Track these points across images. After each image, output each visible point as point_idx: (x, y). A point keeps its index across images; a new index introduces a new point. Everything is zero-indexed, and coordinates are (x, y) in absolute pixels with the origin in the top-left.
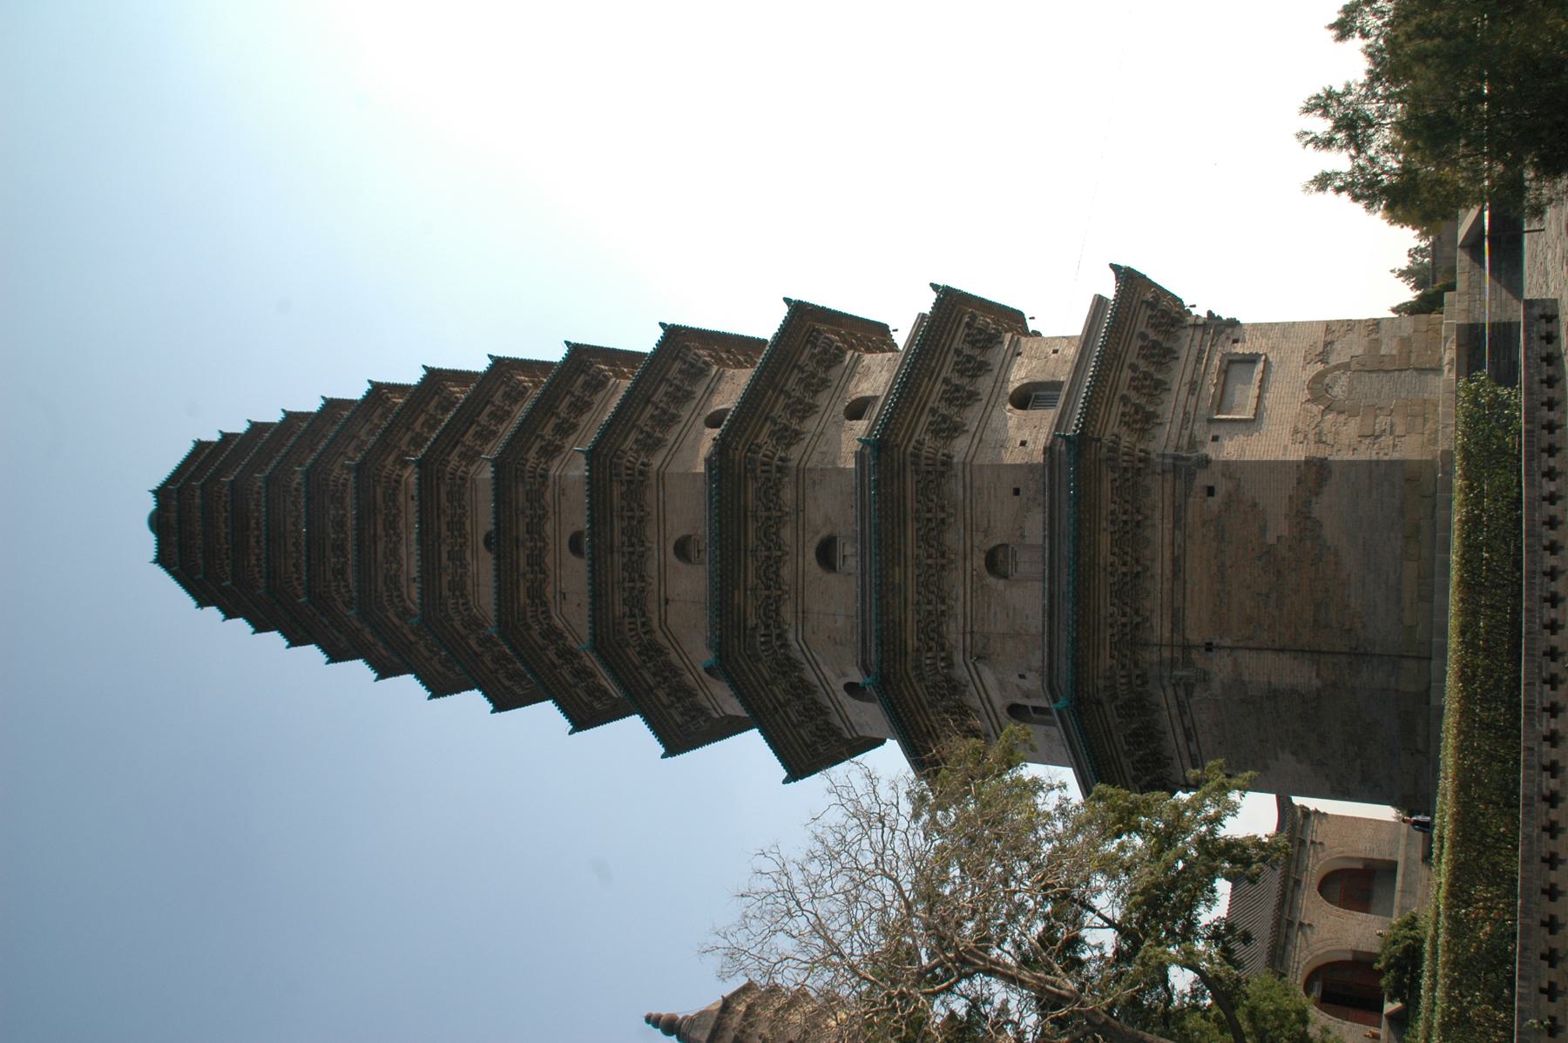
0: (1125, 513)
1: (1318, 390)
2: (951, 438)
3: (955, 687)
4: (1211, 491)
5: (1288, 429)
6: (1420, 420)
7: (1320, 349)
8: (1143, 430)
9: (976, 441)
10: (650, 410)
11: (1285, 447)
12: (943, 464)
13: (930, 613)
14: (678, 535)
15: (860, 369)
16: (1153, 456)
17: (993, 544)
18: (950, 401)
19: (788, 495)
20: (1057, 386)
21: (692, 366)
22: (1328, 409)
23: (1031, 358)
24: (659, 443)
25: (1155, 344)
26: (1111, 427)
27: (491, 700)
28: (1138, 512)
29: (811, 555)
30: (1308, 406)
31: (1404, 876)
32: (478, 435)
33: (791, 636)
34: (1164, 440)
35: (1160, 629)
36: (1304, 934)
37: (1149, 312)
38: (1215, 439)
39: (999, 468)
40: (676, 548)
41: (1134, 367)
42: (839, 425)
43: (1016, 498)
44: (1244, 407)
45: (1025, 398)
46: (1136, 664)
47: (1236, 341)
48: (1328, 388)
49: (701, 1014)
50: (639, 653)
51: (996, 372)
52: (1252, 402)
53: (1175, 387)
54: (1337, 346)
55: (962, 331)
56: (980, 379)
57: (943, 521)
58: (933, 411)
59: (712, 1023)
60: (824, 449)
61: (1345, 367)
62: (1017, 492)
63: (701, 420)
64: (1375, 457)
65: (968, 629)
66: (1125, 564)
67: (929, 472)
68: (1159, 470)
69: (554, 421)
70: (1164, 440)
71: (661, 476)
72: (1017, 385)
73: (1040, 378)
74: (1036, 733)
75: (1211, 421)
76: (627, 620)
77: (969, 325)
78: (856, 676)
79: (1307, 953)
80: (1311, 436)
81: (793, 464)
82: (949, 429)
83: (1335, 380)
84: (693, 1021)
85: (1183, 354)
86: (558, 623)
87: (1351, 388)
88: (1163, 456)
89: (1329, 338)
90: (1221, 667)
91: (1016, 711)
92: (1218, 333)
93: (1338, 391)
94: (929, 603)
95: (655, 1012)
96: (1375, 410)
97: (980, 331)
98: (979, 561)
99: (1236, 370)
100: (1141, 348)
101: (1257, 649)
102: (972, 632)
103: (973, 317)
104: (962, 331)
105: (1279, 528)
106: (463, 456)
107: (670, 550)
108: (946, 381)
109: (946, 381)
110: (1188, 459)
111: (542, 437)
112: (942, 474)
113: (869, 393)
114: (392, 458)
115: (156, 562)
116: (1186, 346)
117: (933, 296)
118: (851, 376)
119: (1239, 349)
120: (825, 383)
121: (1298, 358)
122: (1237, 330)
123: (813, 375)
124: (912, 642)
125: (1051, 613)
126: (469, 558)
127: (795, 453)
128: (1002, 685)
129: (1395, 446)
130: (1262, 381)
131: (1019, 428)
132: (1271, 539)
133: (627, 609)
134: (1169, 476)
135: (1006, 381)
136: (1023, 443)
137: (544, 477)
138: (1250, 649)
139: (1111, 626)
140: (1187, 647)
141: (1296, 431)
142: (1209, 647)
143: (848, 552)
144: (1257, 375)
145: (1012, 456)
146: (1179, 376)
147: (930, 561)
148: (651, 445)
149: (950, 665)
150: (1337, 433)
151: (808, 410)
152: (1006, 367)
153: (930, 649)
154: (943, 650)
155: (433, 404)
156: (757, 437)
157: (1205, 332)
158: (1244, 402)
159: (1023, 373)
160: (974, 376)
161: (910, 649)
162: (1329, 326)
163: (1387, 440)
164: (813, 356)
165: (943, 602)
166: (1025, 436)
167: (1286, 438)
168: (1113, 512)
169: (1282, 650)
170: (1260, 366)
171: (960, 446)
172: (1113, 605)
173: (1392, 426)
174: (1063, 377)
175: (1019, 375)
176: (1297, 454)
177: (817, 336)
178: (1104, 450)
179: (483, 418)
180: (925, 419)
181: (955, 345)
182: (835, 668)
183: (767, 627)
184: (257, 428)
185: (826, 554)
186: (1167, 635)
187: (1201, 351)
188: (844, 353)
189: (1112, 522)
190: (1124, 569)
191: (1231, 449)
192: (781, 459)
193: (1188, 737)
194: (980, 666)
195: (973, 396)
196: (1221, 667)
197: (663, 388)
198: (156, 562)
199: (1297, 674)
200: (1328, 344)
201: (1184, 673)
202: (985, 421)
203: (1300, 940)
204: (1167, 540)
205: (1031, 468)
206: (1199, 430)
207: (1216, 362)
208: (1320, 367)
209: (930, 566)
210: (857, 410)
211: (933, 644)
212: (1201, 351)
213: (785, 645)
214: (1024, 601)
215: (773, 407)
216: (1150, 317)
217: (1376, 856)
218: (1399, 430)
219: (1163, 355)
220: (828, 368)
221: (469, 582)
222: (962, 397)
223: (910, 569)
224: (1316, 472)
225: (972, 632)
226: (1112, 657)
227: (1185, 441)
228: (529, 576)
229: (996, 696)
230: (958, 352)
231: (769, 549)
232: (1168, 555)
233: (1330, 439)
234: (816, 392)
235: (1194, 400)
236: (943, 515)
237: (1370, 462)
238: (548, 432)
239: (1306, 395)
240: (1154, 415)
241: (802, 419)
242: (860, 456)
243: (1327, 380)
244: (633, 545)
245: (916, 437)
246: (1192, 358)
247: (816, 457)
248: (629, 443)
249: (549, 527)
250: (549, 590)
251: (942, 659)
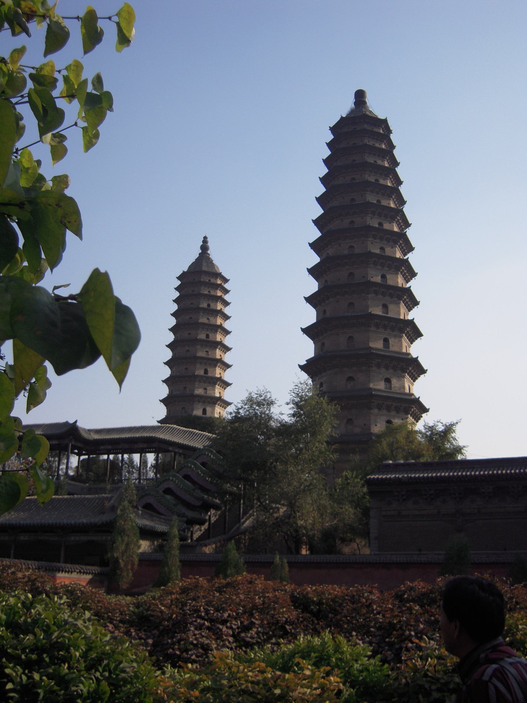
59: (210, 270)
62: (365, 425)
63: (385, 336)
82: (379, 408)
84: (209, 259)
86: (331, 300)
107: (350, 335)
108: (392, 405)
109: (392, 405)
113: (392, 383)
142: (334, 468)
151: (387, 369)
155: (394, 238)
171: (376, 411)
185: (350, 379)
222: (388, 409)
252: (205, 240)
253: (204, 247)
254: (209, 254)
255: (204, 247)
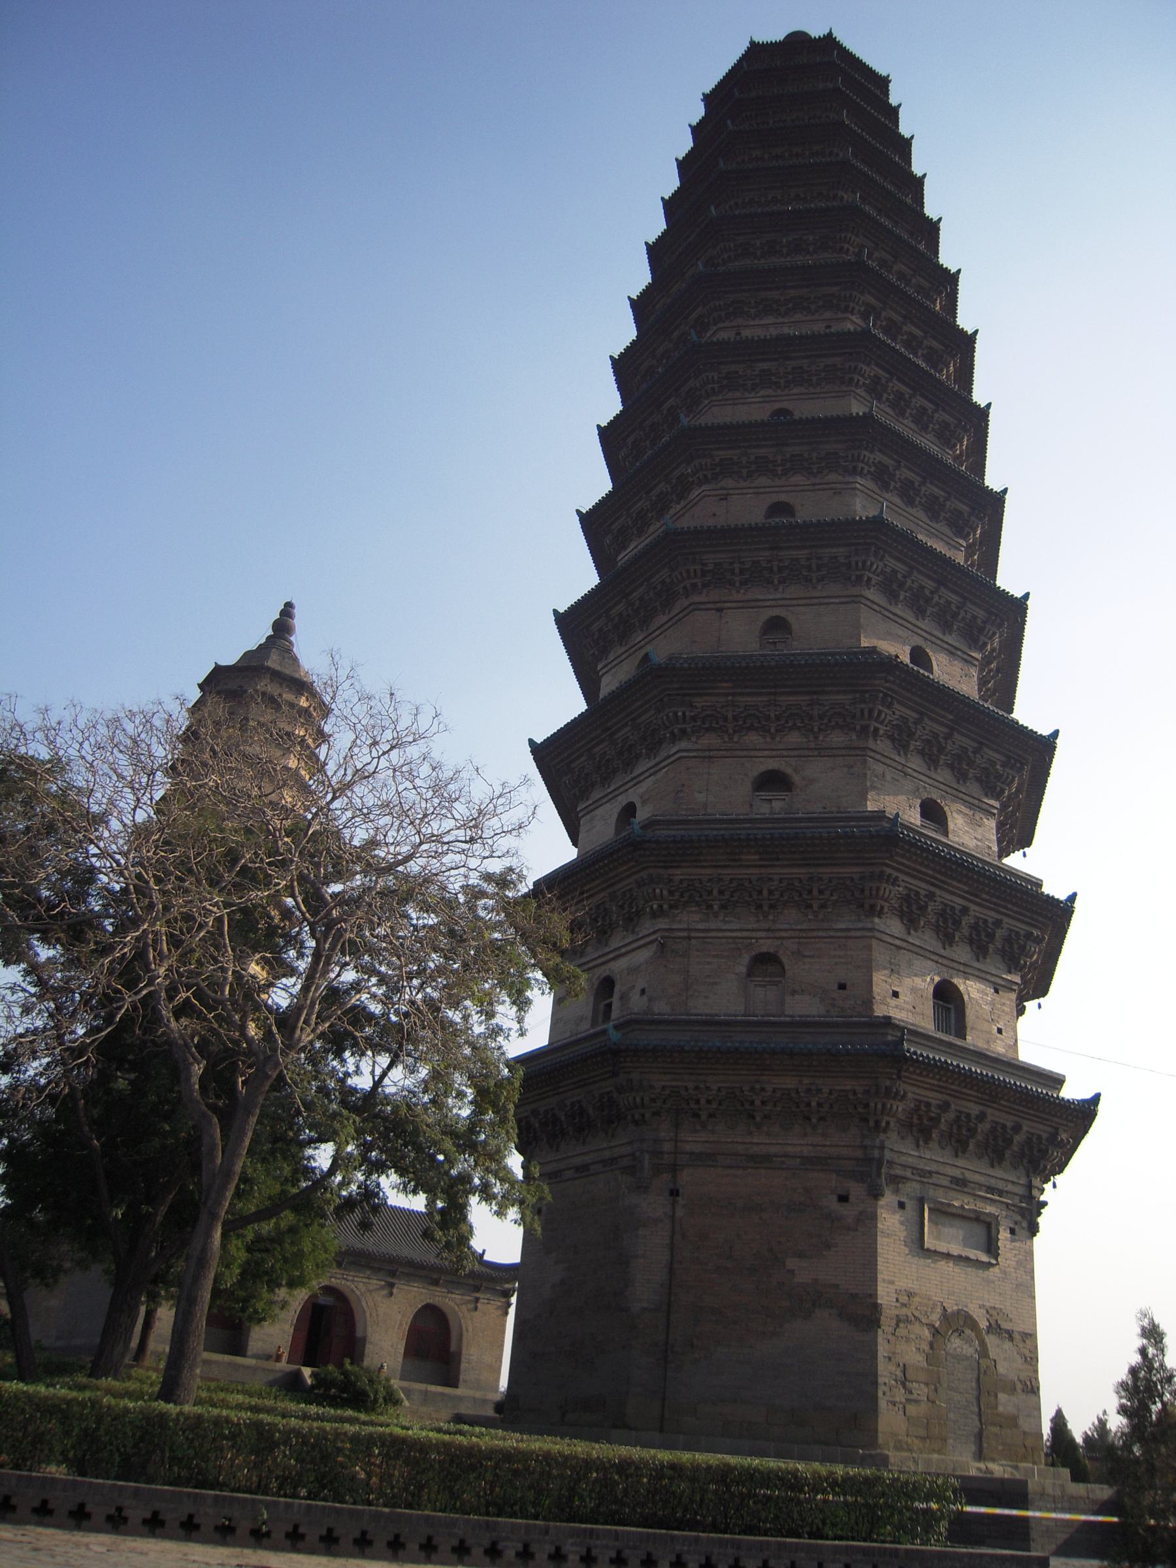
0: (819, 1105)
1: (957, 1322)
2: (901, 915)
3: (631, 921)
4: (843, 1199)
5: (913, 1286)
6: (922, 1433)
7: (1005, 1325)
8: (911, 1125)
9: (897, 942)
10: (930, 585)
11: (892, 1282)
12: (872, 907)
13: (710, 893)
14: (791, 619)
15: (978, 815)
16: (882, 1136)
17: (785, 960)
18: (942, 914)
19: (837, 738)
20: (961, 1033)
21: (981, 630)
22: (936, 1332)
23: (992, 1003)
24: (893, 597)
25: (1009, 1142)
26: (914, 1091)
27: (611, 423)
28: (821, 1119)
29: (772, 764)
30: (939, 1310)
31: (442, 1394)
32: (900, 395)
33: (684, 744)
34: (901, 1150)
35: (694, 1141)
36: (382, 1288)
37: (1044, 1136)
38: (902, 1205)
39: (868, 969)
40: (778, 617)
41: (981, 1117)
42: (916, 792)
43: (836, 986)
44: (938, 1237)
45: (947, 998)
46: (656, 1114)
47: (1012, 1231)
48: (960, 1333)
49: (295, 660)
50: (663, 582)
51: (976, 964)
52: (942, 1247)
53: (960, 1162)
54: (1007, 1345)
55: (1022, 928)
56: (968, 949)
57: (810, 906)
58: (931, 896)
60: (888, 777)
61: (983, 1352)
62: (842, 987)
63: (920, 642)
64: (881, 1380)
65: (693, 934)
66: (763, 1103)
67: (862, 891)
68: (867, 1142)
69: (917, 479)
70: (901, 1150)
71: (856, 600)
72: (961, 988)
73: (970, 1014)
74: (583, 1004)
75: (921, 1201)
76: (698, 567)
77: (1029, 935)
78: (643, 814)
79: (362, 1288)
80: (904, 1311)
81: (871, 743)
83: (969, 1341)
84: (287, 652)
85: (998, 1172)
87: (959, 1358)
88: (882, 1148)
89: (1016, 1336)
90: (653, 1205)
91: (606, 986)
92: (1022, 1212)
93: (955, 1343)
94: (721, 892)
95: (297, 612)
96: (935, 1383)
97: (1023, 948)
98: (767, 946)
99: (980, 1230)
100: (1004, 1126)
101: (672, 1243)
102: (690, 938)
103: (1038, 941)
104: (1022, 928)
105: (803, 1272)
106: (876, 380)
108: (965, 910)
109: (965, 910)
110: (879, 1175)
111: (898, 467)
112: (861, 906)
113: (951, 826)
114: (872, 301)
115: (752, 43)
116: (1007, 1177)
117: (1062, 896)
118: (971, 806)
119: (1004, 1235)
120: (962, 777)
121: (993, 1300)
122: (1026, 1233)
123: (971, 763)
124: (678, 874)
125: (710, 1023)
126: (762, 393)
127: (883, 746)
128: (633, 970)
129: (894, 1404)
130: (967, 1259)
131: (914, 990)
132: (791, 1263)
133: (711, 567)
134: (859, 1153)
135: (966, 975)
136: (896, 994)
137: (854, 472)
138: (672, 1237)
139: (697, 1088)
140: (674, 1168)
141: (910, 1295)
143: (774, 805)
144: (973, 1254)
145: (881, 983)
146: (973, 1168)
147: (765, 893)
148: (891, 587)
149: (654, 915)
150: (908, 1340)
151: (932, 761)
152: (982, 976)
153: (671, 893)
154: (671, 907)
155: (935, 344)
156: (899, 703)
157: (1022, 1198)
158: (946, 1238)
159: (975, 995)
160: (971, 942)
161: (671, 871)
162: (1030, 1337)
163: (900, 1395)
164: (993, 763)
165: (723, 907)
166: (904, 996)
167: (903, 1283)
168: (819, 1091)
169: (671, 1270)
170: (984, 1258)
171: (893, 926)
172: (719, 1089)
173: (917, 1402)
174: (972, 1040)
175: (973, 990)
176: (885, 1295)
177: (1016, 769)
178: (888, 1083)
179: (919, 401)
180: (922, 887)
181: (1006, 920)
182: (649, 792)
183: (694, 719)
184: (904, 146)
185: (773, 781)
186: (688, 1148)
187: (1001, 1193)
188: (997, 798)
189: (808, 1090)
190: (758, 1103)
191: (890, 1222)
192: (876, 730)
193: (582, 1169)
194: (653, 948)
195: (948, 939)
196: (653, 1205)
197: (954, 598)
198: (752, 43)
199: (644, 1289)
200: (1010, 1335)
201: (646, 1162)
202: (921, 952)
203: (375, 1283)
204: (790, 1149)
205: (869, 1001)
206: (912, 1188)
207: (989, 1209)
208: (983, 1324)
209: (760, 892)
210: (933, 813)
211: (677, 894)
212: (1001, 1193)
213: (674, 739)
214: (724, 995)
215: (932, 720)
216: (1040, 1137)
217: (463, 1366)
218: (912, 1409)
219: (996, 1149)
220: (979, 780)
221: (738, 394)
223: (757, 871)
224: (863, 1314)
225: (690, 938)
226: (664, 1088)
227: (898, 1171)
228: (744, 460)
229: (623, 963)
230: (998, 924)
231: (778, 718)
232: (773, 1150)
233: (902, 1331)
234: (951, 767)
235: (946, 1182)
236: (815, 907)
237: (876, 1375)
238: (905, 473)
239: (951, 1308)
240: (928, 1139)
241: (921, 753)
242: (880, 815)
243: (968, 1332)
244: (780, 570)
245: (901, 877)
246: (993, 1182)
247: (879, 768)
248: (893, 564)
249: (798, 479)
250: (729, 482)
251: (661, 906)
252: (288, 610)
253: (283, 626)
254: (291, 642)
255: (283, 626)
